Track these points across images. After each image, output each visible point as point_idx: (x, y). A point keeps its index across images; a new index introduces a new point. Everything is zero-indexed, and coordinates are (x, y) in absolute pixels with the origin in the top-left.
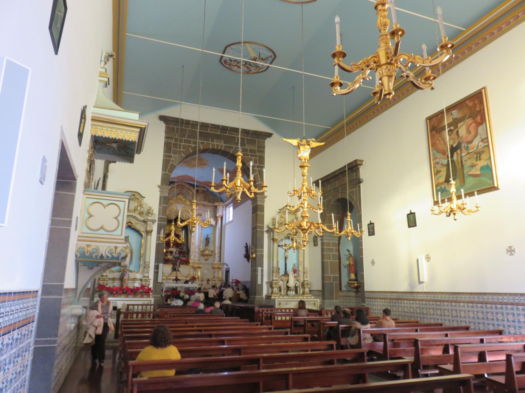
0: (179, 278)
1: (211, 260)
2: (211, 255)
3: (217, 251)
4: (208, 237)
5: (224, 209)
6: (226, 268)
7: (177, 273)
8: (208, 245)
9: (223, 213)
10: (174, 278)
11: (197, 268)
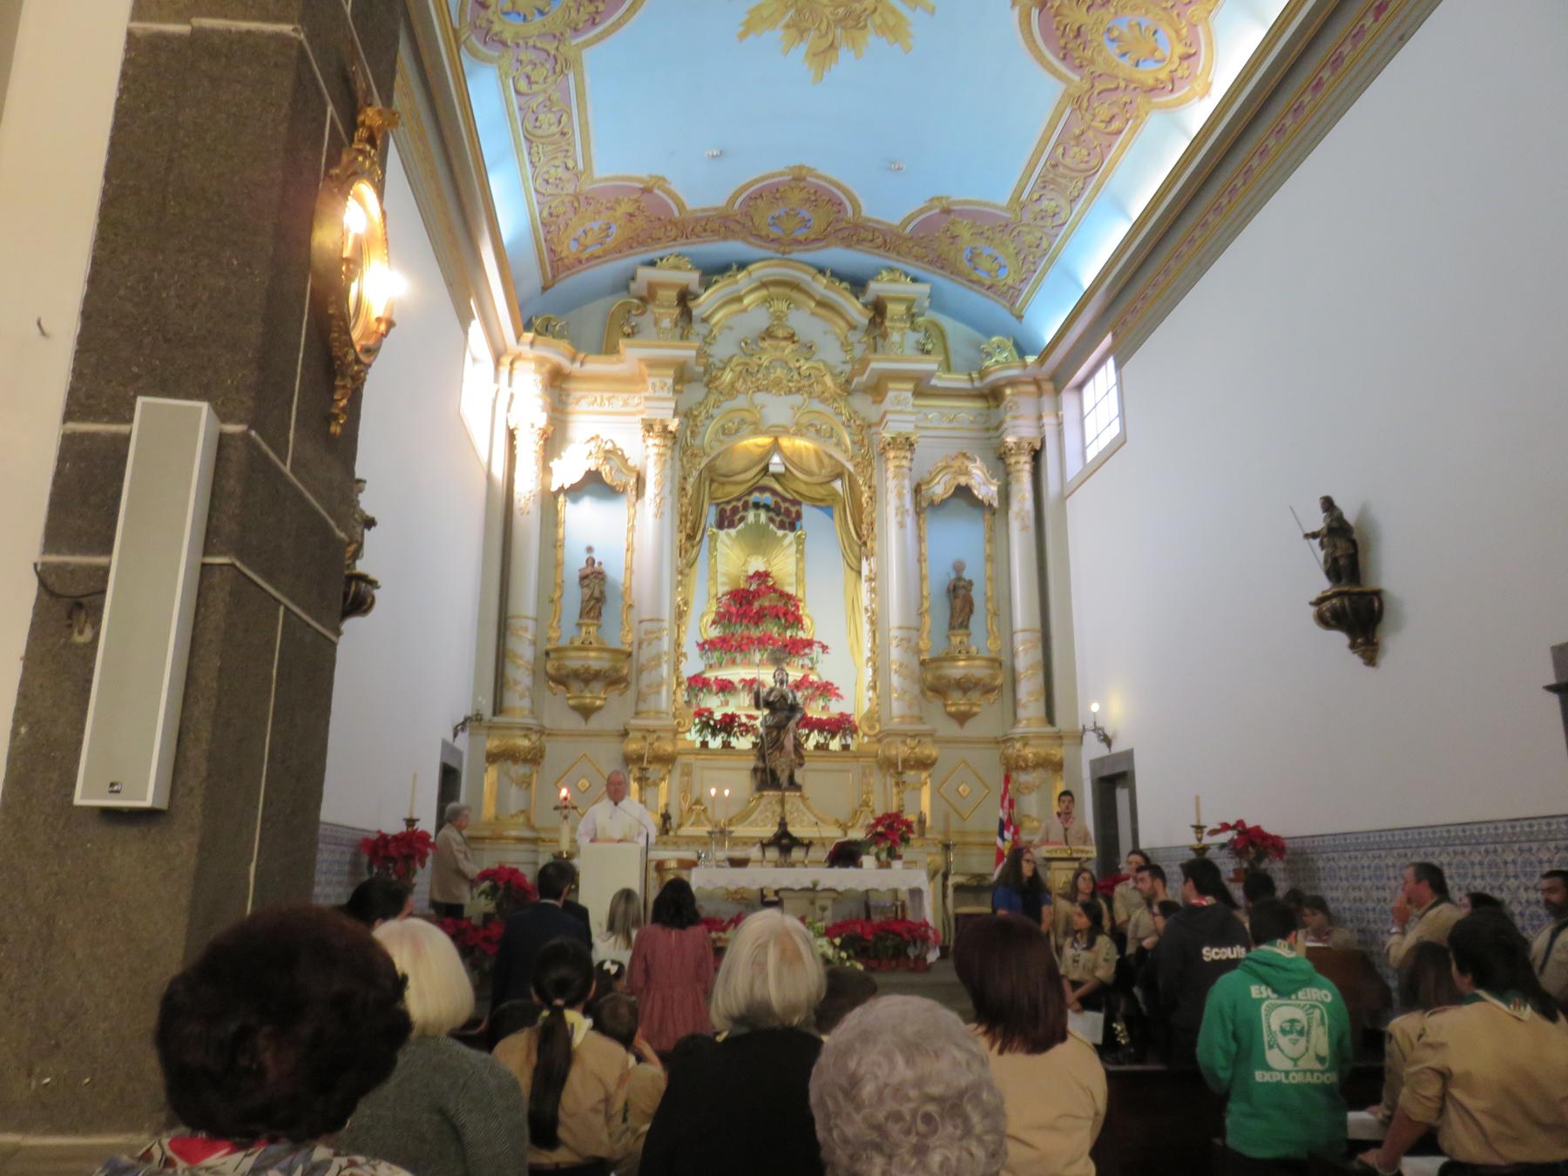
0: (796, 830)
1: (987, 722)
2: (988, 690)
3: (1026, 658)
4: (959, 579)
5: (1047, 401)
6: (1096, 764)
7: (782, 802)
8: (964, 625)
9: (1041, 427)
10: (769, 831)
11: (905, 761)
